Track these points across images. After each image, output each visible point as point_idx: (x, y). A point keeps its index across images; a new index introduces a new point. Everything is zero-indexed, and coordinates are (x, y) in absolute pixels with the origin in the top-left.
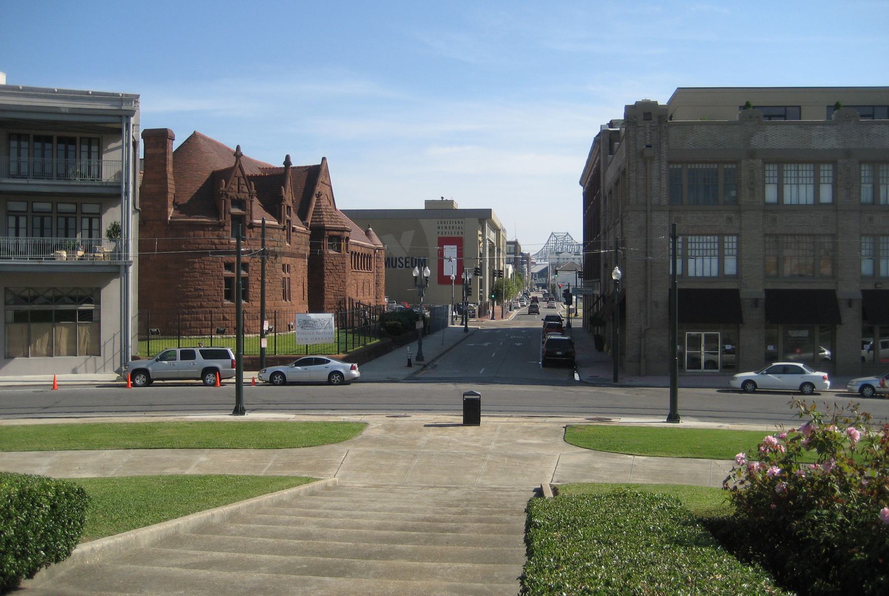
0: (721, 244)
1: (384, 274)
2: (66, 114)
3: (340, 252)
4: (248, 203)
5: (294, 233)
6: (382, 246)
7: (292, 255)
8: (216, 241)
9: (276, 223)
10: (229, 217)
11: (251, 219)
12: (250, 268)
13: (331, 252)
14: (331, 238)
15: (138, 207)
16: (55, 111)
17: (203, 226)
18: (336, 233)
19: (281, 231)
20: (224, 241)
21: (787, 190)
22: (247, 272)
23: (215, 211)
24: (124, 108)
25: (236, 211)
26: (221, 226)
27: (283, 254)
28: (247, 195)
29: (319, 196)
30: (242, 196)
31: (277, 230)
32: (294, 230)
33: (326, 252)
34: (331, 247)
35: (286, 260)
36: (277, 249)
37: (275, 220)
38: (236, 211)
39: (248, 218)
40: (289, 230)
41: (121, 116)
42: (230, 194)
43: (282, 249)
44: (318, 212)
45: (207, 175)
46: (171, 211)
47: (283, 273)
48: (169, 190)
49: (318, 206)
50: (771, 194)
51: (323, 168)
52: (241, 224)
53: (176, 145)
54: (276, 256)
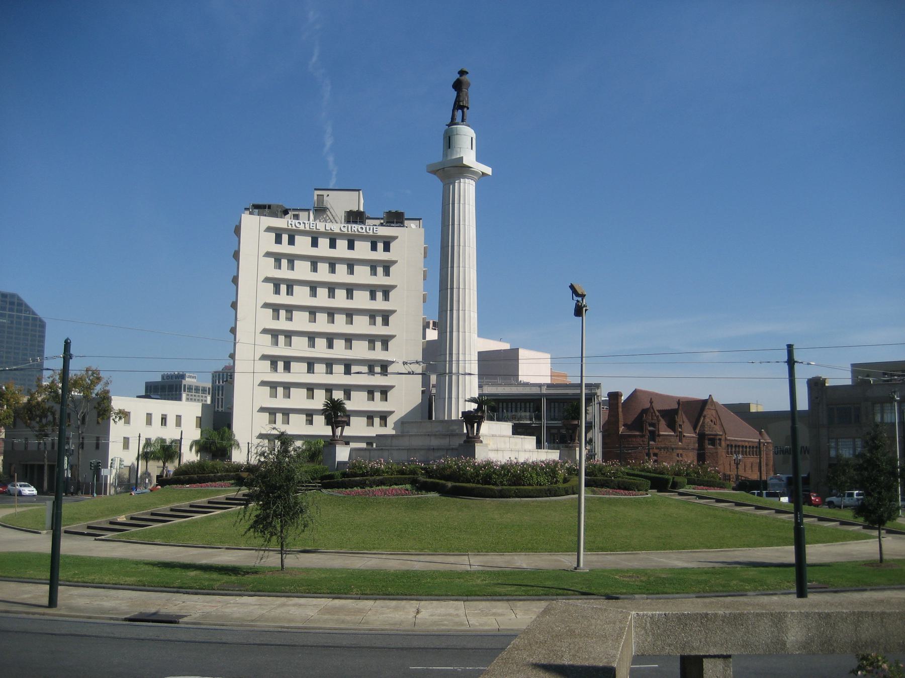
0: (854, 442)
1: (772, 458)
2: (571, 395)
3: (714, 446)
4: (657, 425)
5: (685, 438)
6: (770, 441)
7: (683, 449)
8: (642, 443)
9: (673, 434)
10: (647, 432)
11: (659, 432)
12: (659, 456)
13: (710, 447)
14: (710, 440)
15: (601, 430)
16: (567, 394)
17: (635, 436)
18: (712, 437)
19: (675, 437)
20: (645, 443)
21: (885, 416)
22: (657, 457)
23: (641, 429)
24: (593, 392)
25: (651, 428)
26: (642, 436)
27: (677, 449)
28: (656, 421)
29: (704, 417)
30: (653, 421)
31: (673, 437)
32: (684, 436)
33: (706, 447)
34: (709, 444)
35: (680, 452)
36: (673, 446)
37: (670, 430)
38: (651, 428)
39: (657, 432)
40: (681, 437)
41: (592, 395)
42: (648, 421)
43: (676, 446)
44: (703, 426)
45: (639, 411)
46: (621, 429)
47: (678, 458)
48: (620, 420)
49: (703, 422)
50: (878, 418)
51: (709, 401)
52: (653, 436)
53: (623, 398)
54: (673, 450)
